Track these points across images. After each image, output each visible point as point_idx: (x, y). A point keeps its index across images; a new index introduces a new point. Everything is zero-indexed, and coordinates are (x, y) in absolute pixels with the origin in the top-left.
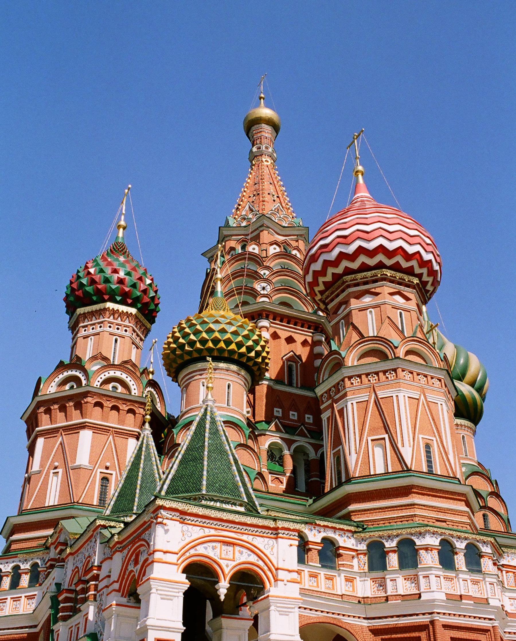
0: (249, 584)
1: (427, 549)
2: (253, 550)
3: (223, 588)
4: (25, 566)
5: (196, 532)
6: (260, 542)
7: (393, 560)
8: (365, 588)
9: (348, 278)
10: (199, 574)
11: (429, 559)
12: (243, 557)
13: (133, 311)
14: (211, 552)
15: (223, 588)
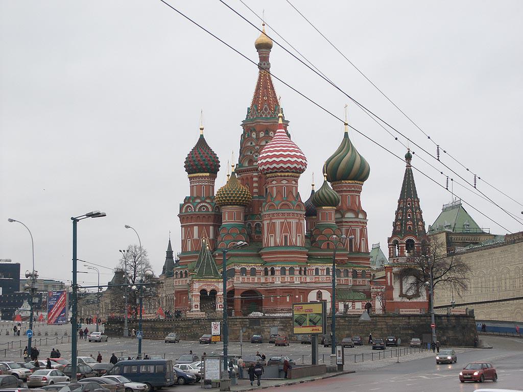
0: (214, 292)
1: (278, 270)
2: (214, 286)
3: (208, 293)
4: (183, 272)
5: (202, 284)
6: (216, 284)
7: (270, 273)
8: (263, 280)
9: (268, 175)
10: (203, 292)
11: (277, 273)
12: (212, 288)
13: (208, 174)
14: (205, 287)
15: (208, 293)
